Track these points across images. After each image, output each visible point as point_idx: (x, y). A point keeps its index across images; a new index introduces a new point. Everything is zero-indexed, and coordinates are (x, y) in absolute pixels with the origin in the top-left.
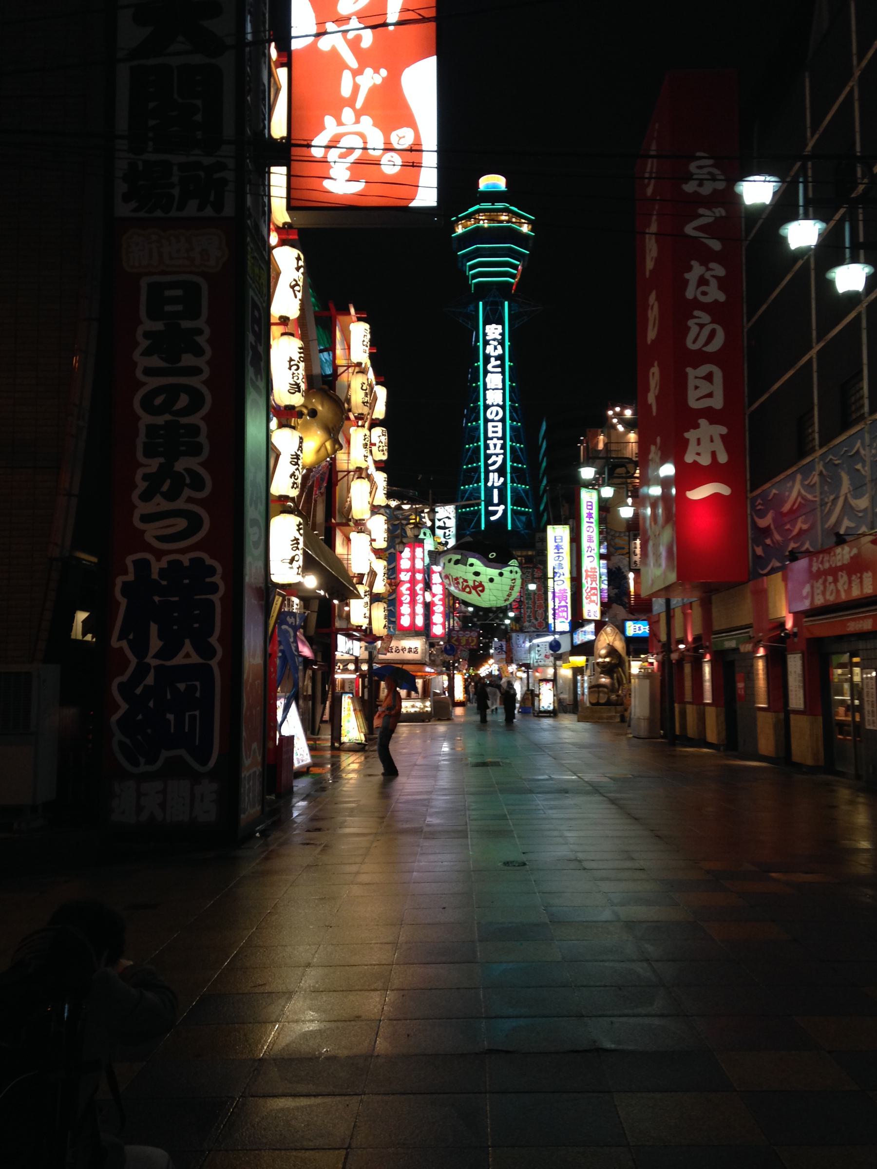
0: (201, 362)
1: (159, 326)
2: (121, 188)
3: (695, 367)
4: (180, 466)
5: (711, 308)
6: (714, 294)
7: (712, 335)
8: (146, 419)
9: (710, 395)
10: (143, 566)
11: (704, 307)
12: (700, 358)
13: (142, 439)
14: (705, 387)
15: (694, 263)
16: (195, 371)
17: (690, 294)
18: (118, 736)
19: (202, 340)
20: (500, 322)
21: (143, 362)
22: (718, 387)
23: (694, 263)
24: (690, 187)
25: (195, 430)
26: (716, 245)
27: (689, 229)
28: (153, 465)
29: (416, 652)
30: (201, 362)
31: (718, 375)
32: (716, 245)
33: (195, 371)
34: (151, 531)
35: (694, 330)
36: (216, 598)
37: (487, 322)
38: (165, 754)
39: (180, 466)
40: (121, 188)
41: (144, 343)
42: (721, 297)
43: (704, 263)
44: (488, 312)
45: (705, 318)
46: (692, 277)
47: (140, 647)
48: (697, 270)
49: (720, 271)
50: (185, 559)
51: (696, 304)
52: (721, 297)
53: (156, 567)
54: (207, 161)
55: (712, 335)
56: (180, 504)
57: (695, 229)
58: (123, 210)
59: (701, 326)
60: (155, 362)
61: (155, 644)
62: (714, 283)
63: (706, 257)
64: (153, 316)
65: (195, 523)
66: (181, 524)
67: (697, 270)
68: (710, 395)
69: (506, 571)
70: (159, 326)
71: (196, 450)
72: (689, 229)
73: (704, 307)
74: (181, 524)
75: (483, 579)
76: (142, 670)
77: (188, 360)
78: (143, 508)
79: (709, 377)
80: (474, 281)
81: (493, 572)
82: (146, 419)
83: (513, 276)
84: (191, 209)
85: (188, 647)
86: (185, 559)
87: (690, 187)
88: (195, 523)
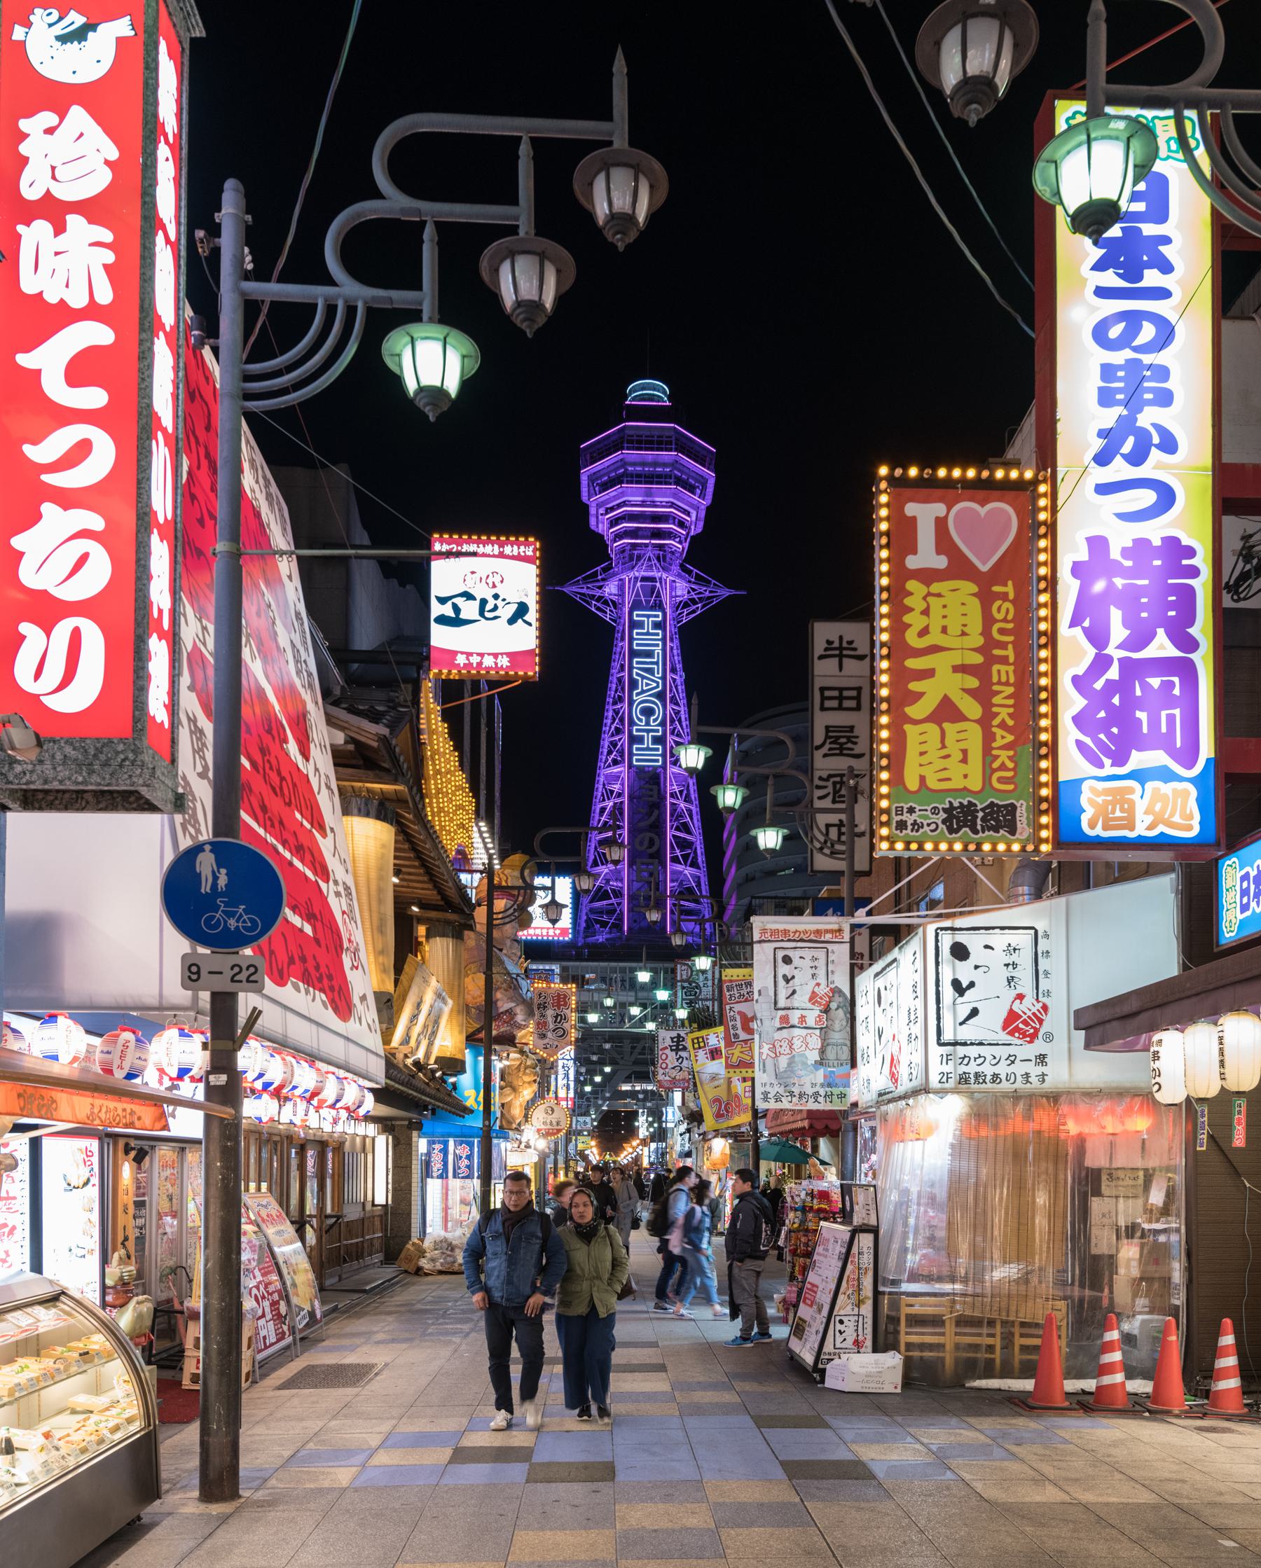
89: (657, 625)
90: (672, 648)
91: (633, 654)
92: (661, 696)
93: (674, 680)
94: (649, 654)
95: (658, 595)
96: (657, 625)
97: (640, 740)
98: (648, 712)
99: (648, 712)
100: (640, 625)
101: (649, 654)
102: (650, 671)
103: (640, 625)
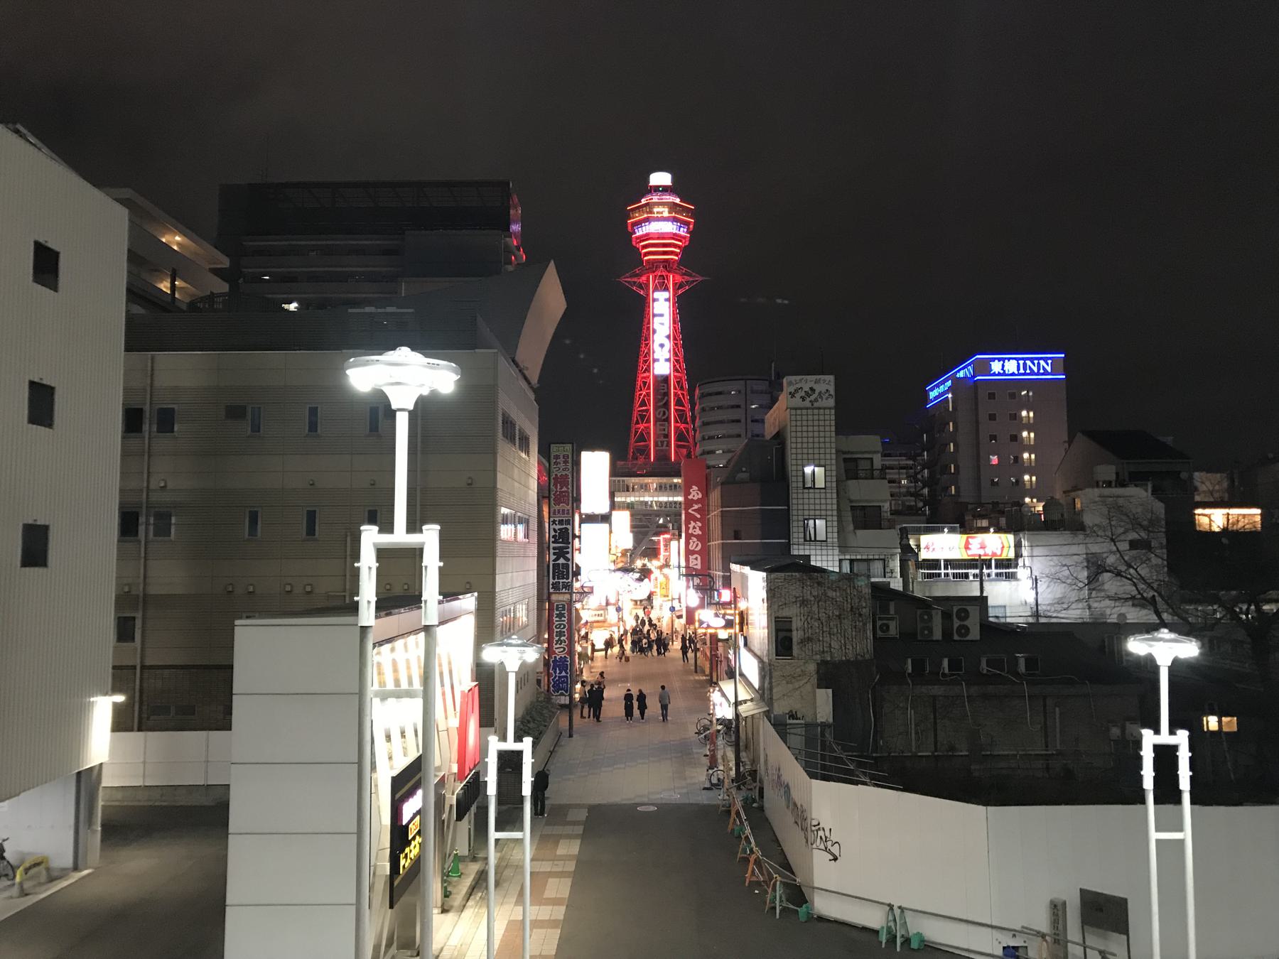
0: (565, 619)
1: (558, 612)
2: (551, 586)
3: (692, 555)
4: (562, 638)
5: (697, 536)
6: (698, 532)
7: (697, 545)
8: (556, 630)
9: (696, 565)
10: (555, 657)
11: (695, 536)
12: (693, 552)
13: (555, 634)
14: (695, 562)
15: (692, 522)
16: (564, 621)
17: (690, 532)
18: (552, 688)
19: (566, 615)
20: (667, 289)
21: (555, 619)
22: (699, 561)
23: (692, 522)
24: (690, 497)
25: (564, 632)
26: (699, 516)
27: (690, 511)
28: (557, 638)
29: (601, 615)
30: (565, 619)
31: (699, 558)
32: (699, 516)
33: (564, 621)
34: (557, 651)
35: (691, 545)
36: (568, 663)
37: (655, 289)
38: (560, 692)
39: (562, 638)
40: (551, 586)
41: (555, 616)
42: (700, 533)
43: (695, 522)
44: (656, 285)
45: (695, 539)
46: (691, 526)
47: (555, 673)
48: (693, 523)
49: (700, 524)
50: (563, 656)
51: (692, 535)
52: (700, 533)
53: (558, 657)
54: (567, 581)
55: (697, 545)
56: (562, 646)
57: (693, 510)
58: (551, 591)
59: (694, 542)
60: (557, 619)
61: (558, 672)
62: (698, 528)
63: (695, 520)
64: (557, 610)
65: (565, 649)
66: (562, 649)
67: (693, 523)
68: (696, 565)
69: (642, 584)
70: (558, 612)
71: (565, 636)
72: (690, 511)
73: (695, 536)
74: (562, 649)
75: (632, 588)
76: (556, 677)
77: (563, 619)
78: (556, 646)
79: (696, 559)
80: (646, 258)
81: (637, 584)
82: (556, 630)
83: (677, 254)
84: (564, 590)
85: (564, 672)
86: (563, 656)
87: (690, 497)
88: (565, 649)
89: (666, 300)
90: (673, 311)
91: (654, 315)
92: (668, 337)
93: (674, 327)
94: (661, 315)
95: (666, 285)
96: (666, 300)
97: (658, 360)
98: (662, 346)
99: (662, 346)
100: (657, 300)
101: (661, 315)
102: (662, 324)
103: (657, 300)
